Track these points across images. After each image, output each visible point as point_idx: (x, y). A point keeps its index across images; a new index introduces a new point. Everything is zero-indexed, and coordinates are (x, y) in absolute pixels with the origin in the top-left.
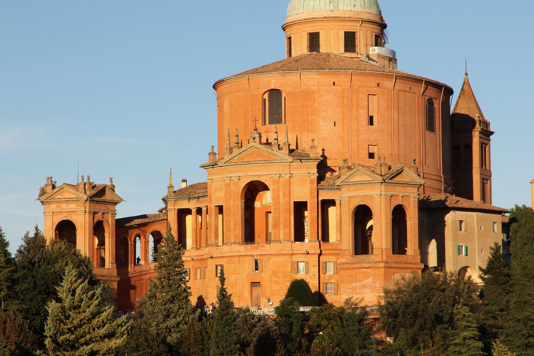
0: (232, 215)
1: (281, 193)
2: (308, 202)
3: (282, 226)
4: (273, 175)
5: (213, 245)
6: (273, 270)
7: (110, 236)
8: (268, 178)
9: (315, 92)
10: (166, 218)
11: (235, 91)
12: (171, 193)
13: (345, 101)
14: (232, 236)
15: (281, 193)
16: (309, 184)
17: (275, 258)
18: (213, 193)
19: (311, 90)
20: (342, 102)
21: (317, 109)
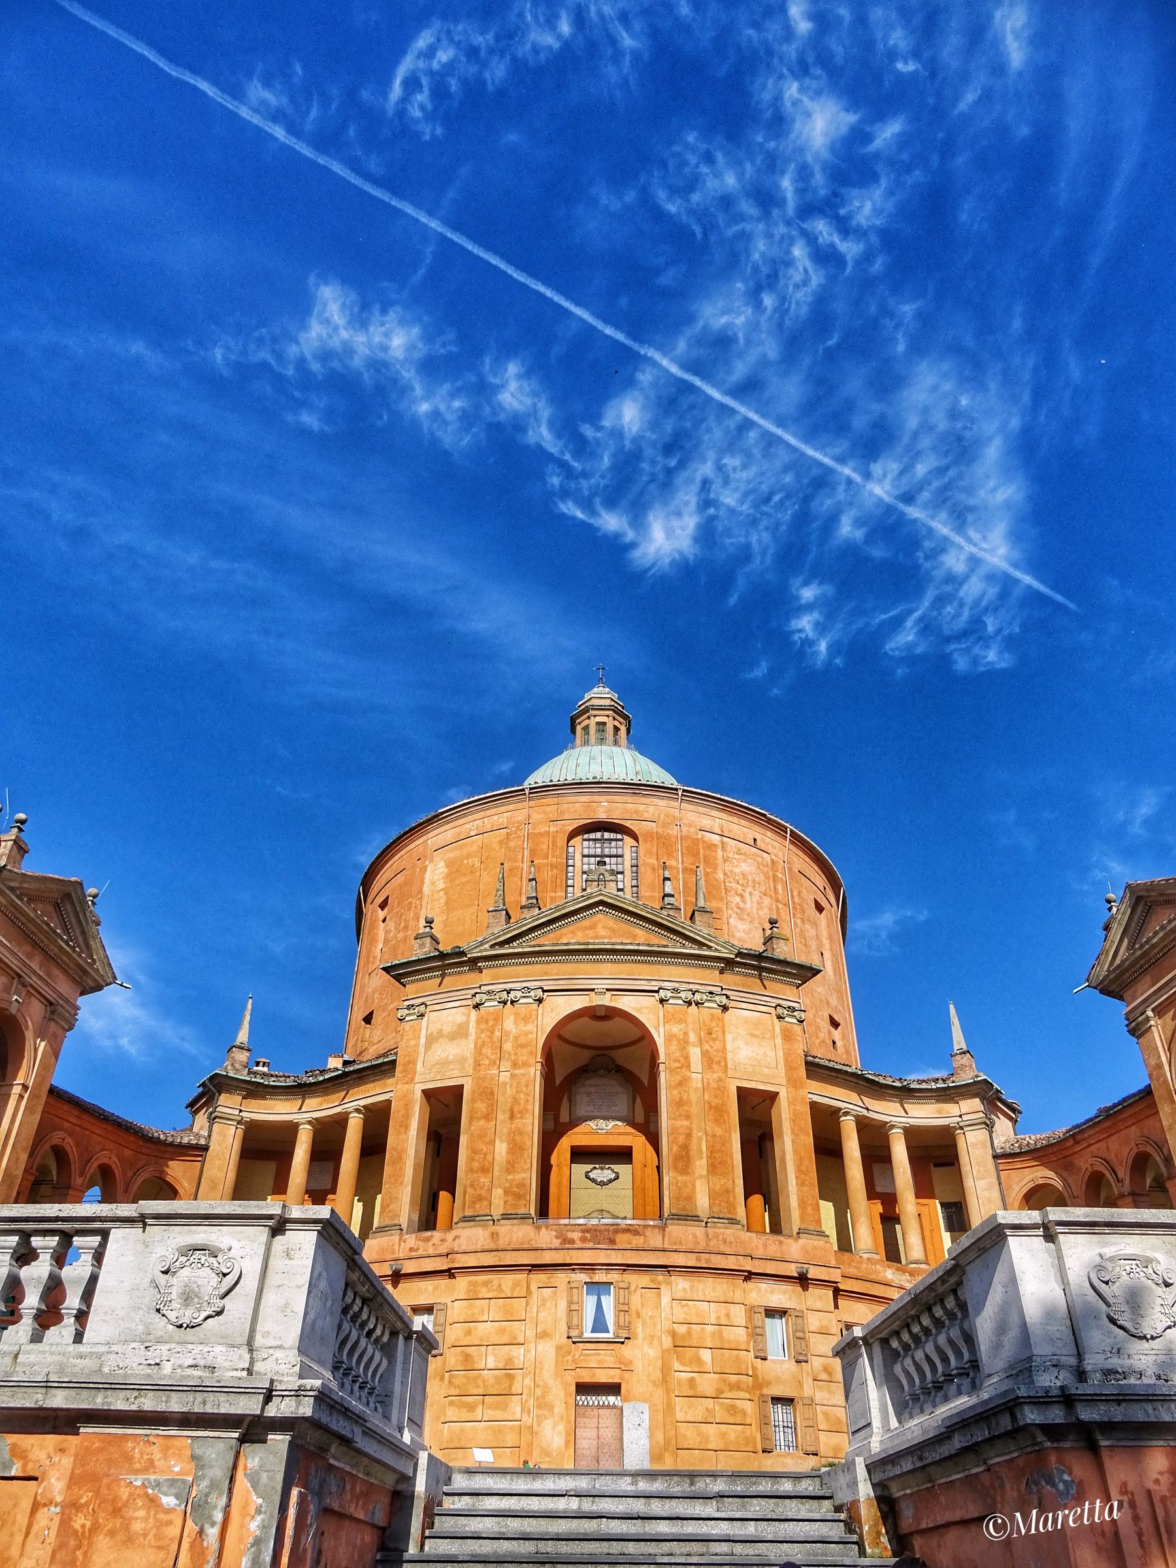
0: (501, 1116)
1: (695, 1053)
2: (781, 1095)
3: (700, 1165)
4: (669, 994)
5: (401, 1230)
6: (673, 1334)
7: (25, 1100)
8: (650, 1001)
9: (716, 846)
10: (203, 1142)
11: (473, 833)
12: (237, 1066)
13: (780, 887)
14: (498, 1192)
15: (695, 1053)
16: (779, 1040)
17: (681, 1284)
18: (422, 1050)
19: (706, 839)
20: (775, 889)
21: (723, 886)
